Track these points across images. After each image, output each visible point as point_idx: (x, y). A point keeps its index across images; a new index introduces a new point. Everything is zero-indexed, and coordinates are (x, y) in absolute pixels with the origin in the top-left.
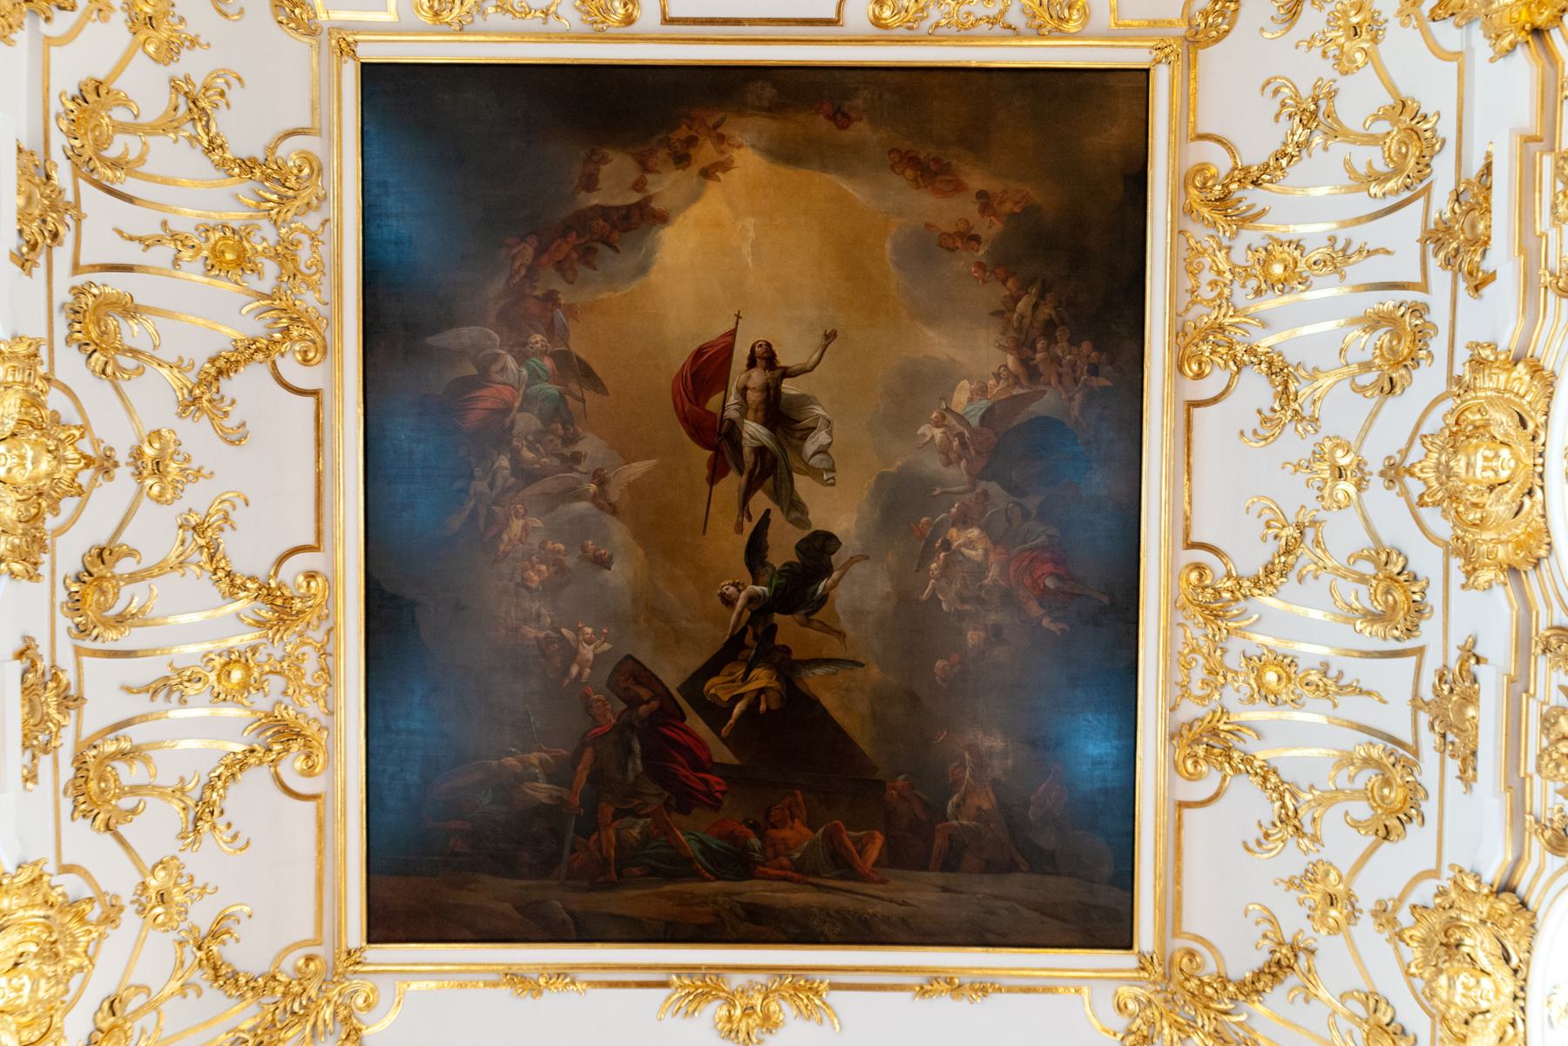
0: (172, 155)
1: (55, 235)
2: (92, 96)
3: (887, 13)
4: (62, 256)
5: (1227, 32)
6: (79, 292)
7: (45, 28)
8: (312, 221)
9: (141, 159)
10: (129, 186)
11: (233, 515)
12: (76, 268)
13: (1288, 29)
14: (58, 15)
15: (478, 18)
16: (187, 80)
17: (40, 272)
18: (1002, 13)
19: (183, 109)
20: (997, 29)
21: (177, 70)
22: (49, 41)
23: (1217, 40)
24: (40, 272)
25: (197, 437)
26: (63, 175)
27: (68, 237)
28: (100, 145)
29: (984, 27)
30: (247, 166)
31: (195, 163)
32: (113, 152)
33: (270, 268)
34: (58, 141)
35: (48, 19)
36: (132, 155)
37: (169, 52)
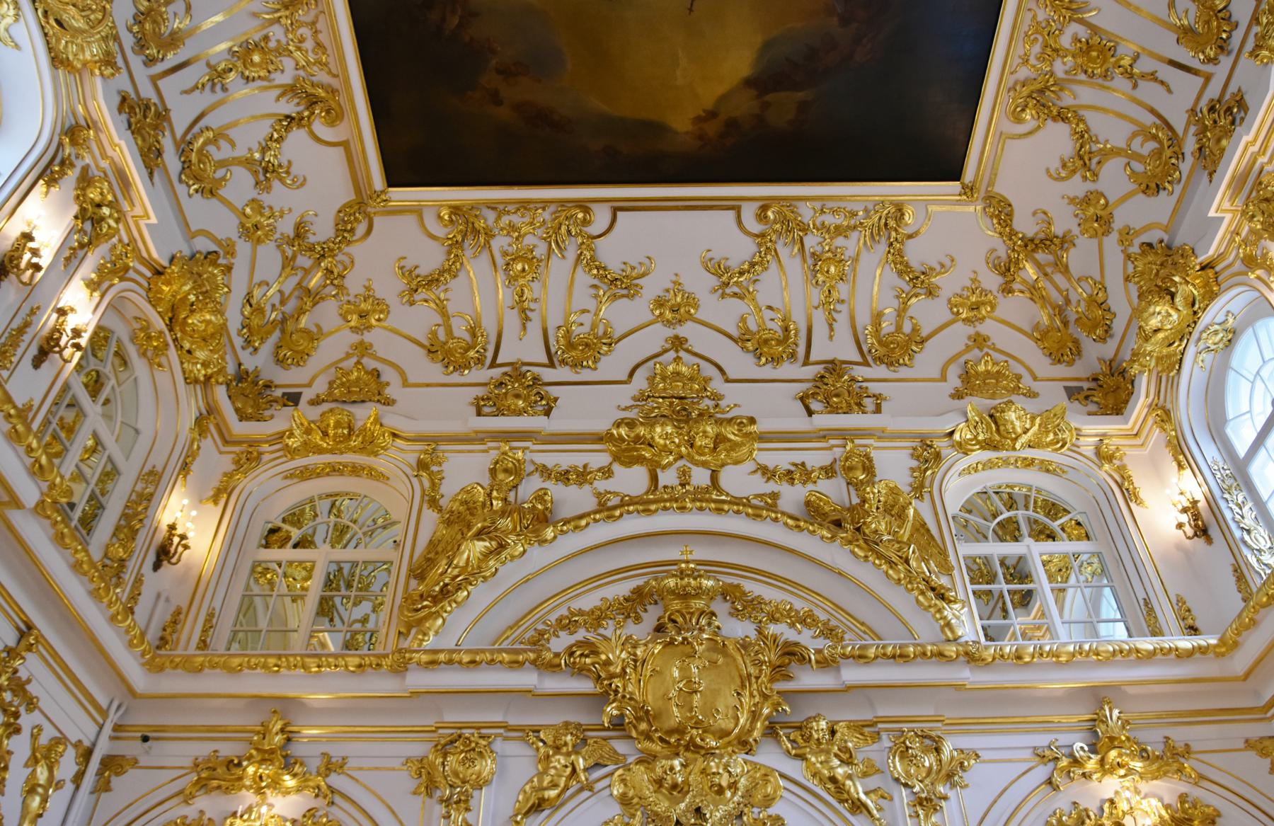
1: (1212, 109)
2: (1152, 187)
3: (580, 215)
5: (340, 212)
9: (1134, 135)
10: (1149, 119)
13: (302, 216)
14: (1154, 241)
15: (870, 207)
16: (1085, 178)
17: (1232, 88)
18: (499, 217)
19: (1095, 161)
20: (501, 207)
21: (1089, 186)
23: (345, 206)
24: (1232, 88)
26: (1190, 145)
27: (1204, 104)
28: (1158, 153)
29: (511, 208)
32: (1152, 145)
34: (1185, 167)
35: (1161, 241)
36: (1139, 140)
37: (1087, 200)
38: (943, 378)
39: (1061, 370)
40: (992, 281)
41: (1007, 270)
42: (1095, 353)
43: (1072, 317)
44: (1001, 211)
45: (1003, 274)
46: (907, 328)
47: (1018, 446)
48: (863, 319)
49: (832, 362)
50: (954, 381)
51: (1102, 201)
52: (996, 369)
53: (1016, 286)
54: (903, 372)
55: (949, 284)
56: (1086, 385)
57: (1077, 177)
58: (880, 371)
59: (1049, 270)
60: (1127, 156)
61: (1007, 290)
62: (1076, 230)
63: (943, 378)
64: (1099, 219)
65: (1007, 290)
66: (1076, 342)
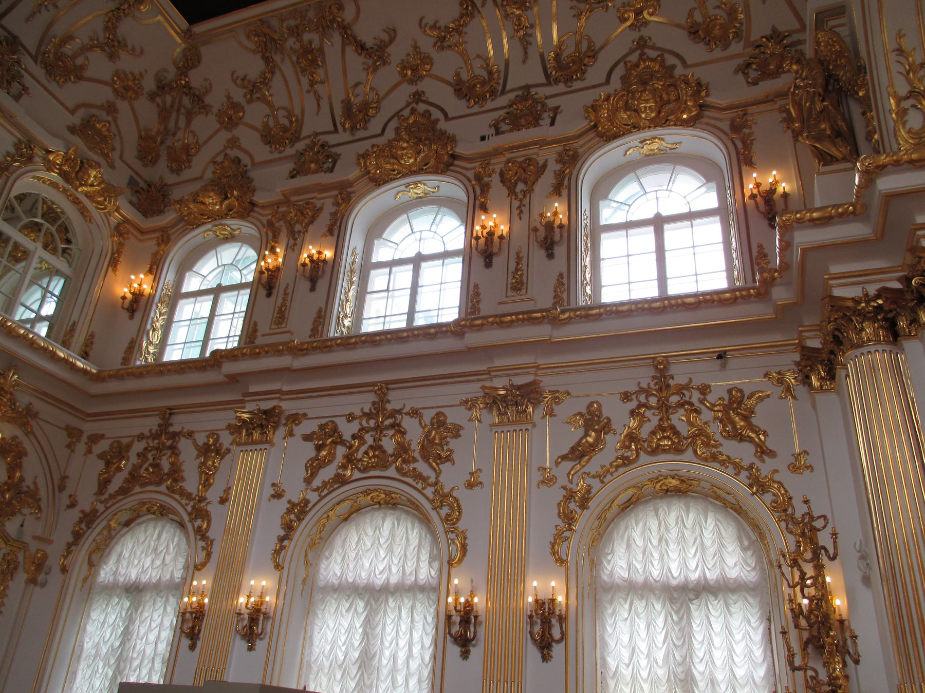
0: (277, 93)
4: (332, 139)
6: (345, 130)
7: (249, 167)
8: (275, 23)
9: (284, 108)
11: (431, 23)
12: (336, 130)
19: (258, 95)
22: (253, 164)
25: (398, 52)
30: (267, 60)
31: (277, 82)
32: (287, 123)
33: (306, 37)
36: (285, 113)
37: (236, 107)
38: (73, 112)
39: (137, 165)
40: (149, 84)
41: (163, 87)
42: (161, 172)
43: (168, 143)
44: (191, 60)
45: (158, 87)
46: (79, 61)
47: (80, 190)
48: (59, 29)
49: (15, 37)
50: (76, 119)
51: (241, 114)
52: (106, 133)
53: (159, 100)
54: (53, 87)
55: (127, 63)
56: (142, 184)
57: (243, 91)
58: (40, 72)
59: (182, 110)
60: (273, 113)
61: (152, 97)
62: (215, 110)
63: (73, 112)
64: (230, 118)
65: (152, 97)
66: (158, 156)
